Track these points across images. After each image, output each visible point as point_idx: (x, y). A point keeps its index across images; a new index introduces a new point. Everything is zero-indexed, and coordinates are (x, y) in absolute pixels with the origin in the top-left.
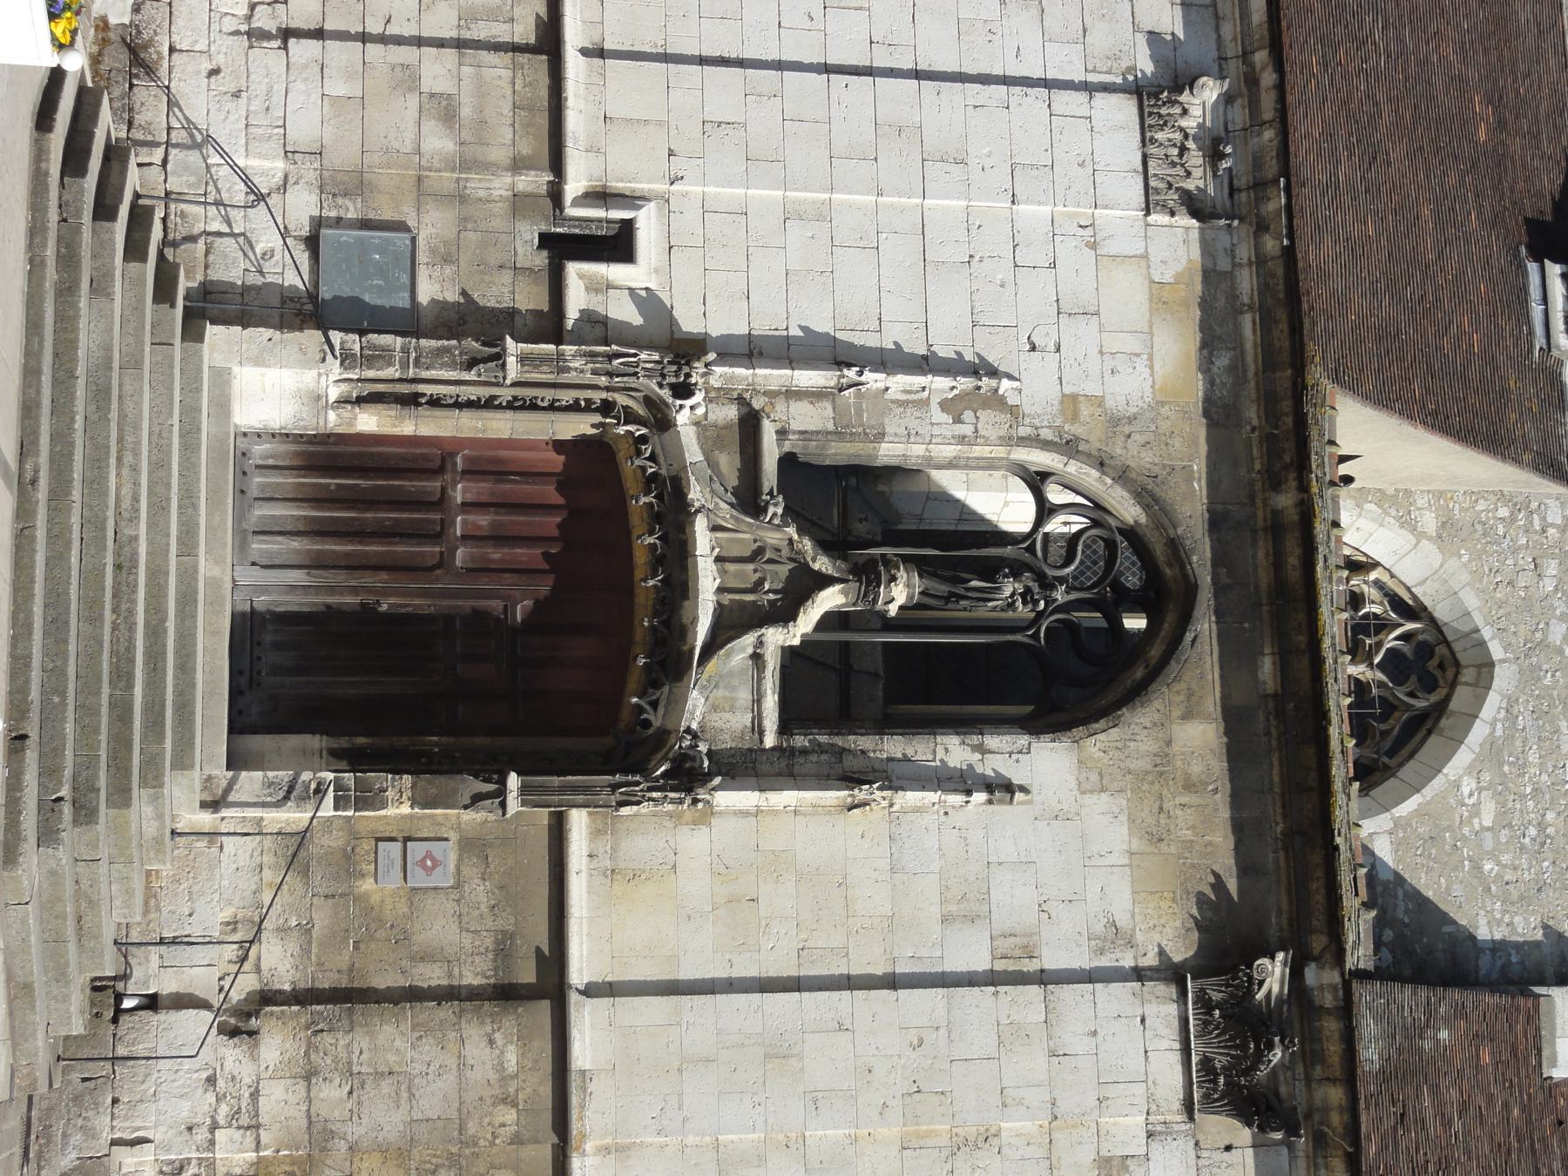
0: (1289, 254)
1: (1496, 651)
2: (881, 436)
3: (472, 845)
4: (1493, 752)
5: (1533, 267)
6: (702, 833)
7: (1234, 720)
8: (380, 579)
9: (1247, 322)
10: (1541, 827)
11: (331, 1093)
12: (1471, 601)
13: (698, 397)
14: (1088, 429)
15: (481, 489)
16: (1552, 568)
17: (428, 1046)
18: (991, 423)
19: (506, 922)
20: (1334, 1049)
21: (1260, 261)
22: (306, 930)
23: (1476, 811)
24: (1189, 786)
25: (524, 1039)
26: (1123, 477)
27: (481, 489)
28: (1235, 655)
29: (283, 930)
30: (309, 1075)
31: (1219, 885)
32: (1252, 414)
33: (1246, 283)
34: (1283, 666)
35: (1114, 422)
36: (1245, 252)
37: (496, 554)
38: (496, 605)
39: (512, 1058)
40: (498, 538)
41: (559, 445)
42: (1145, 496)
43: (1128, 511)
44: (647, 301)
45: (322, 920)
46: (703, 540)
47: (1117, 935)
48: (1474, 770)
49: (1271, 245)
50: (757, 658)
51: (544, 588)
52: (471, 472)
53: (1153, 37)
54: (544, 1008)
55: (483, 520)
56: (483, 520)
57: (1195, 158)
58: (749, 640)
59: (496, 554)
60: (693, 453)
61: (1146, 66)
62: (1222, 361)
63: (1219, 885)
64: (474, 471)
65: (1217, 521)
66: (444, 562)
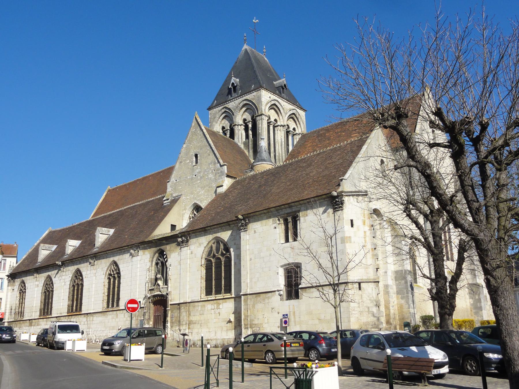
0: (139, 243)
1: (193, 203)
2: (151, 278)
3: (172, 312)
4: (201, 202)
5: (164, 205)
6: (172, 292)
7: (167, 244)
8: (161, 321)
9: (145, 245)
10: (207, 195)
11: (184, 323)
12: (190, 206)
13: (148, 295)
14: (151, 260)
15: (156, 312)
16: (188, 197)
17: (182, 315)
18: (150, 268)
19: (176, 308)
20: (183, 234)
21: (141, 245)
22: (176, 326)
23: (205, 203)
24: (171, 248)
25: (182, 307)
26: (154, 256)
27: (156, 312)
28: (164, 244)
29: (176, 328)
30: (183, 325)
31: (176, 245)
32: (150, 244)
33: (143, 246)
34: (164, 240)
35: (150, 257)
36: (141, 246)
37: (160, 311)
38: (163, 311)
39: (183, 308)
40: (159, 311)
41: (154, 306)
42: (155, 254)
43: (157, 255)
44: (144, 299)
45: (175, 325)
46: (156, 294)
47: (179, 254)
48: (202, 204)
49: (139, 245)
50: (162, 288)
51: (162, 306)
52: (155, 313)
53: (130, 256)
54: (180, 305)
55: (158, 312)
56: (158, 312)
57: (136, 252)
58: (161, 289)
59: (160, 311)
60: (151, 295)
61: (131, 257)
62: (147, 248)
63: (176, 245)
64: (155, 313)
65: (156, 247)
66: (160, 315)
